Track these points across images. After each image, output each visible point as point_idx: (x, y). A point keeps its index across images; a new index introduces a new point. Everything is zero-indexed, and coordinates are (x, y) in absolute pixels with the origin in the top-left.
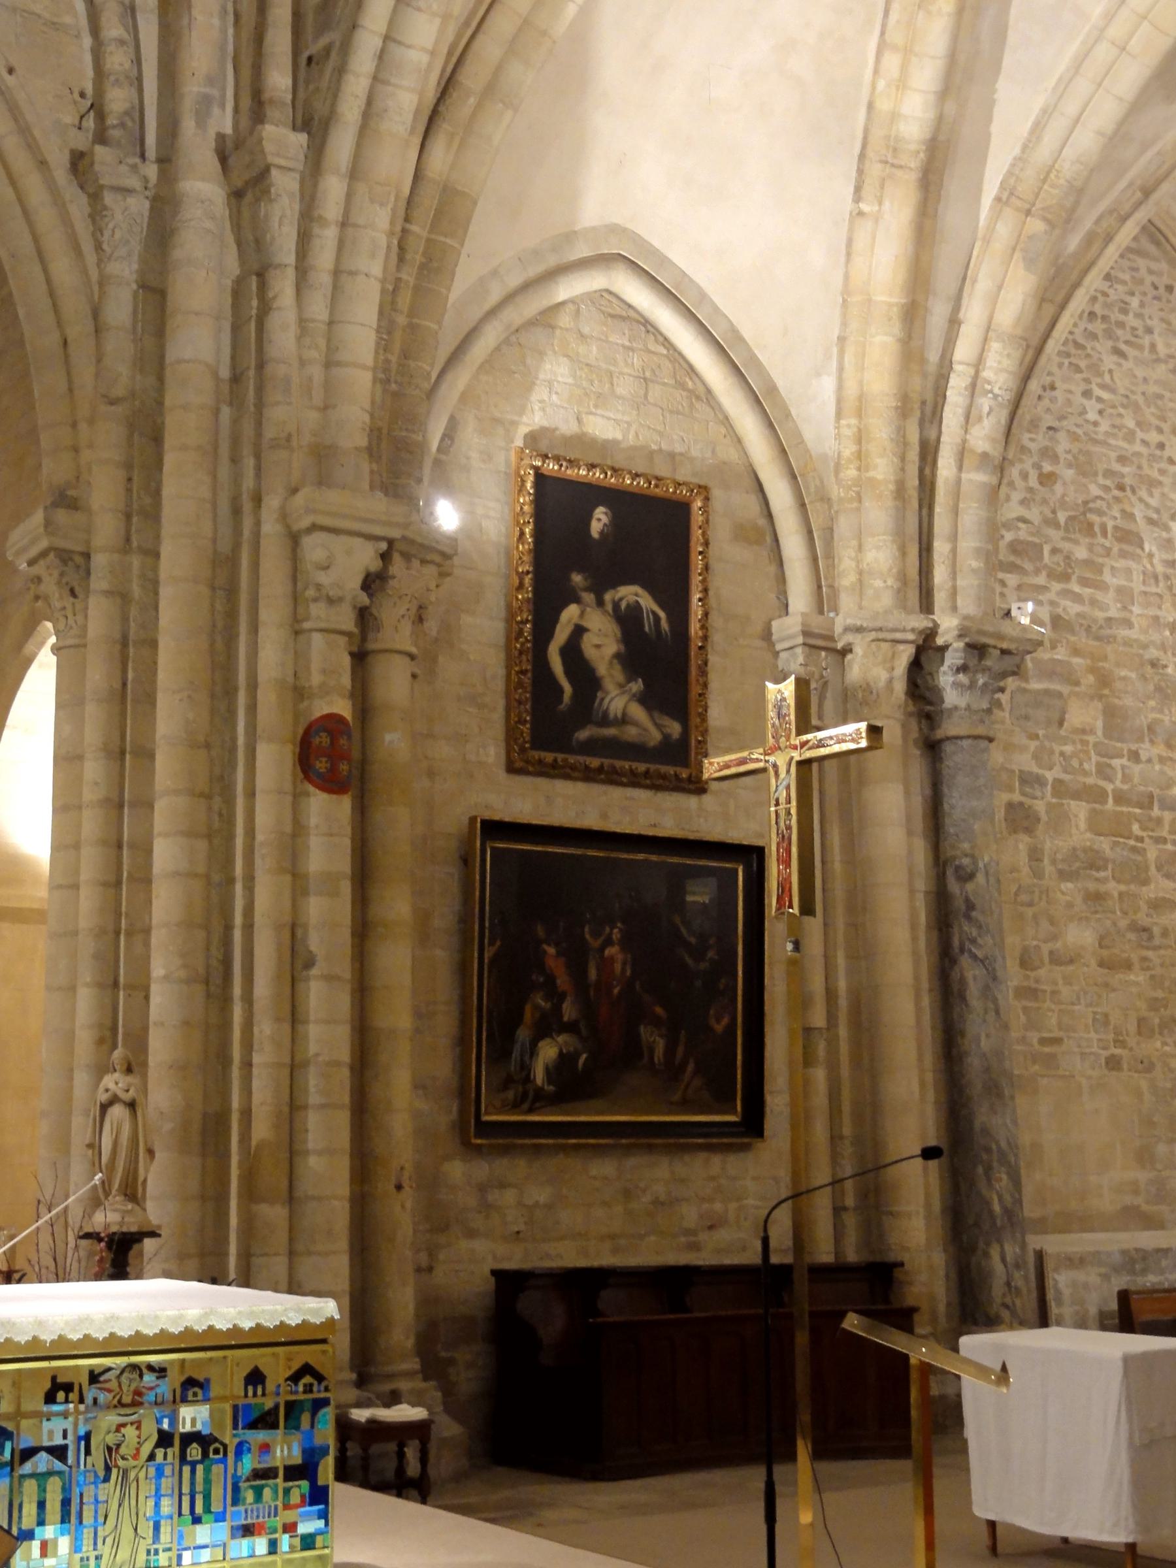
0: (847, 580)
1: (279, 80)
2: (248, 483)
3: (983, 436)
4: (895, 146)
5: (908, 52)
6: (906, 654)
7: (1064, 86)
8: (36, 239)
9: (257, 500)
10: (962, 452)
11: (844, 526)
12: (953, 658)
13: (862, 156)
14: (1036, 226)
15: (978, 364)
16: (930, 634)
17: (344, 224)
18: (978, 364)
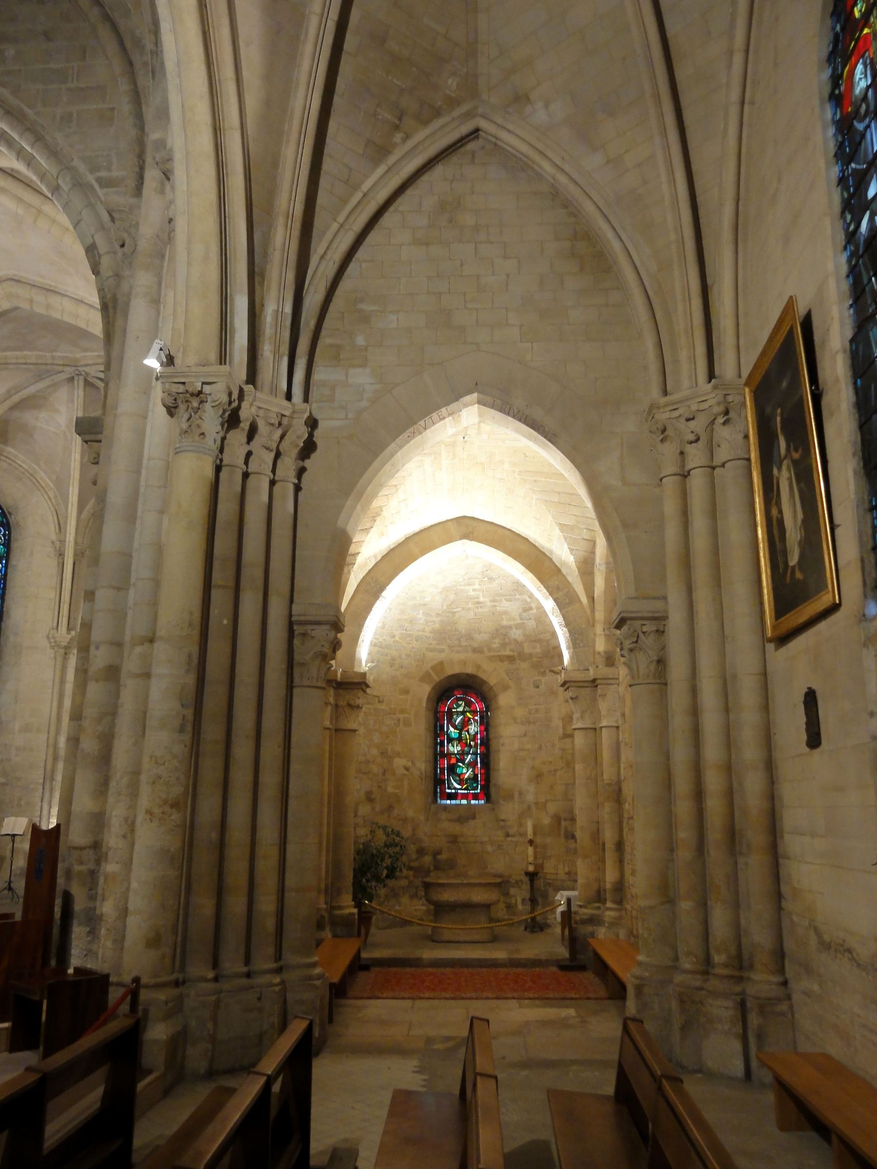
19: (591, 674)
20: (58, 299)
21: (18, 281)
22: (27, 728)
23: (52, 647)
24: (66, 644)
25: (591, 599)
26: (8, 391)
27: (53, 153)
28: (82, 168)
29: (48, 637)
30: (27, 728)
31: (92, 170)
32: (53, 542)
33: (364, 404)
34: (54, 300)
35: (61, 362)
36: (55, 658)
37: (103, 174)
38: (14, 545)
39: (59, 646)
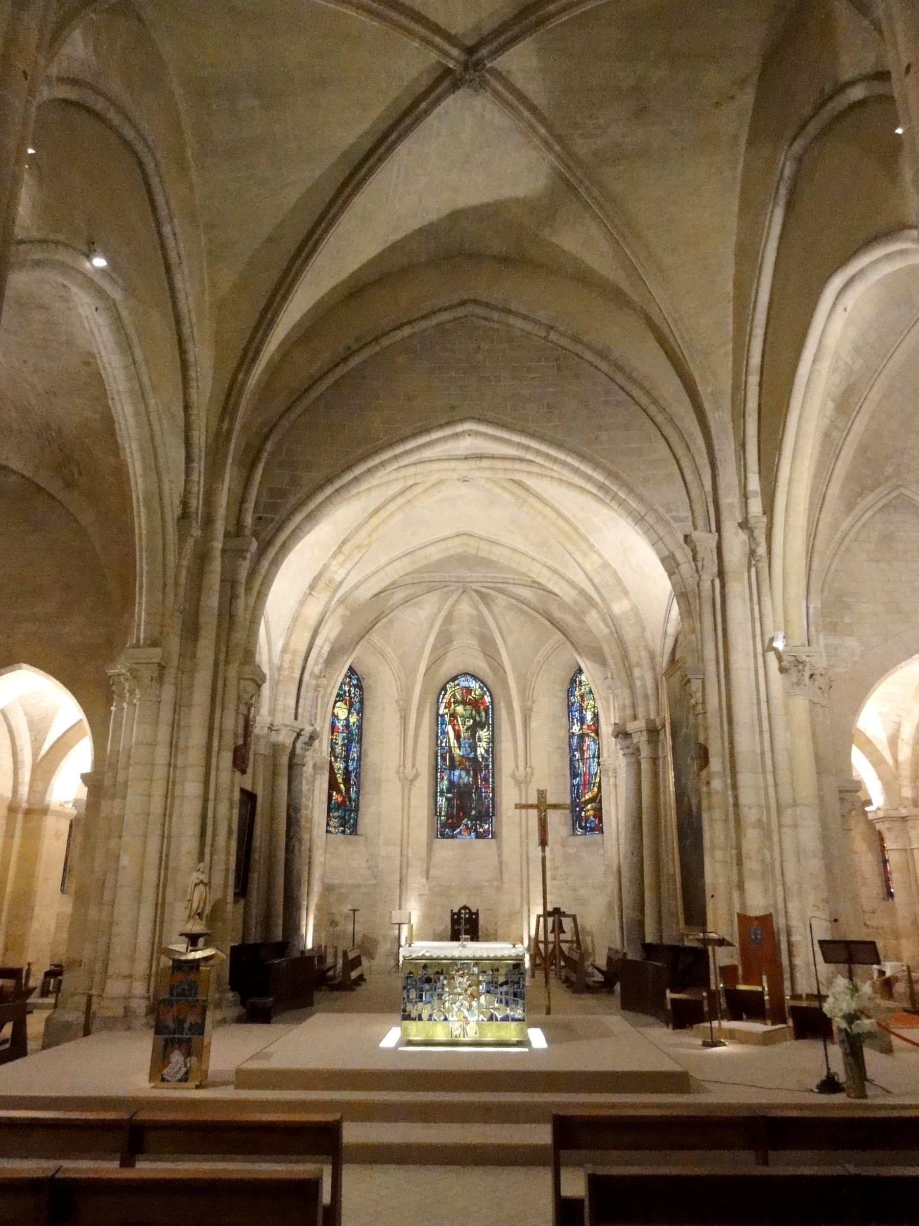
0: (280, 707)
1: (249, 520)
2: (222, 657)
3: (317, 670)
4: (331, 581)
5: (347, 557)
6: (295, 734)
7: (367, 578)
8: (164, 545)
9: (227, 662)
10: (312, 674)
11: (281, 688)
12: (302, 739)
13: (317, 579)
14: (348, 613)
15: (321, 648)
16: (302, 730)
17: (265, 577)
18: (321, 648)
19: (904, 812)
20: (500, 548)
21: (471, 536)
22: (387, 843)
23: (400, 780)
24: (410, 778)
25: (896, 761)
26: (405, 598)
27: (641, 499)
28: (661, 510)
29: (398, 772)
30: (387, 843)
31: (669, 510)
32: (397, 701)
33: (856, 658)
34: (497, 550)
35: (454, 579)
36: (403, 788)
37: (675, 514)
38: (366, 703)
39: (406, 779)
